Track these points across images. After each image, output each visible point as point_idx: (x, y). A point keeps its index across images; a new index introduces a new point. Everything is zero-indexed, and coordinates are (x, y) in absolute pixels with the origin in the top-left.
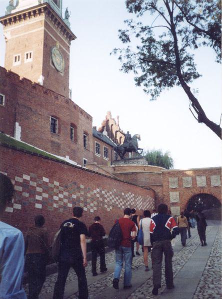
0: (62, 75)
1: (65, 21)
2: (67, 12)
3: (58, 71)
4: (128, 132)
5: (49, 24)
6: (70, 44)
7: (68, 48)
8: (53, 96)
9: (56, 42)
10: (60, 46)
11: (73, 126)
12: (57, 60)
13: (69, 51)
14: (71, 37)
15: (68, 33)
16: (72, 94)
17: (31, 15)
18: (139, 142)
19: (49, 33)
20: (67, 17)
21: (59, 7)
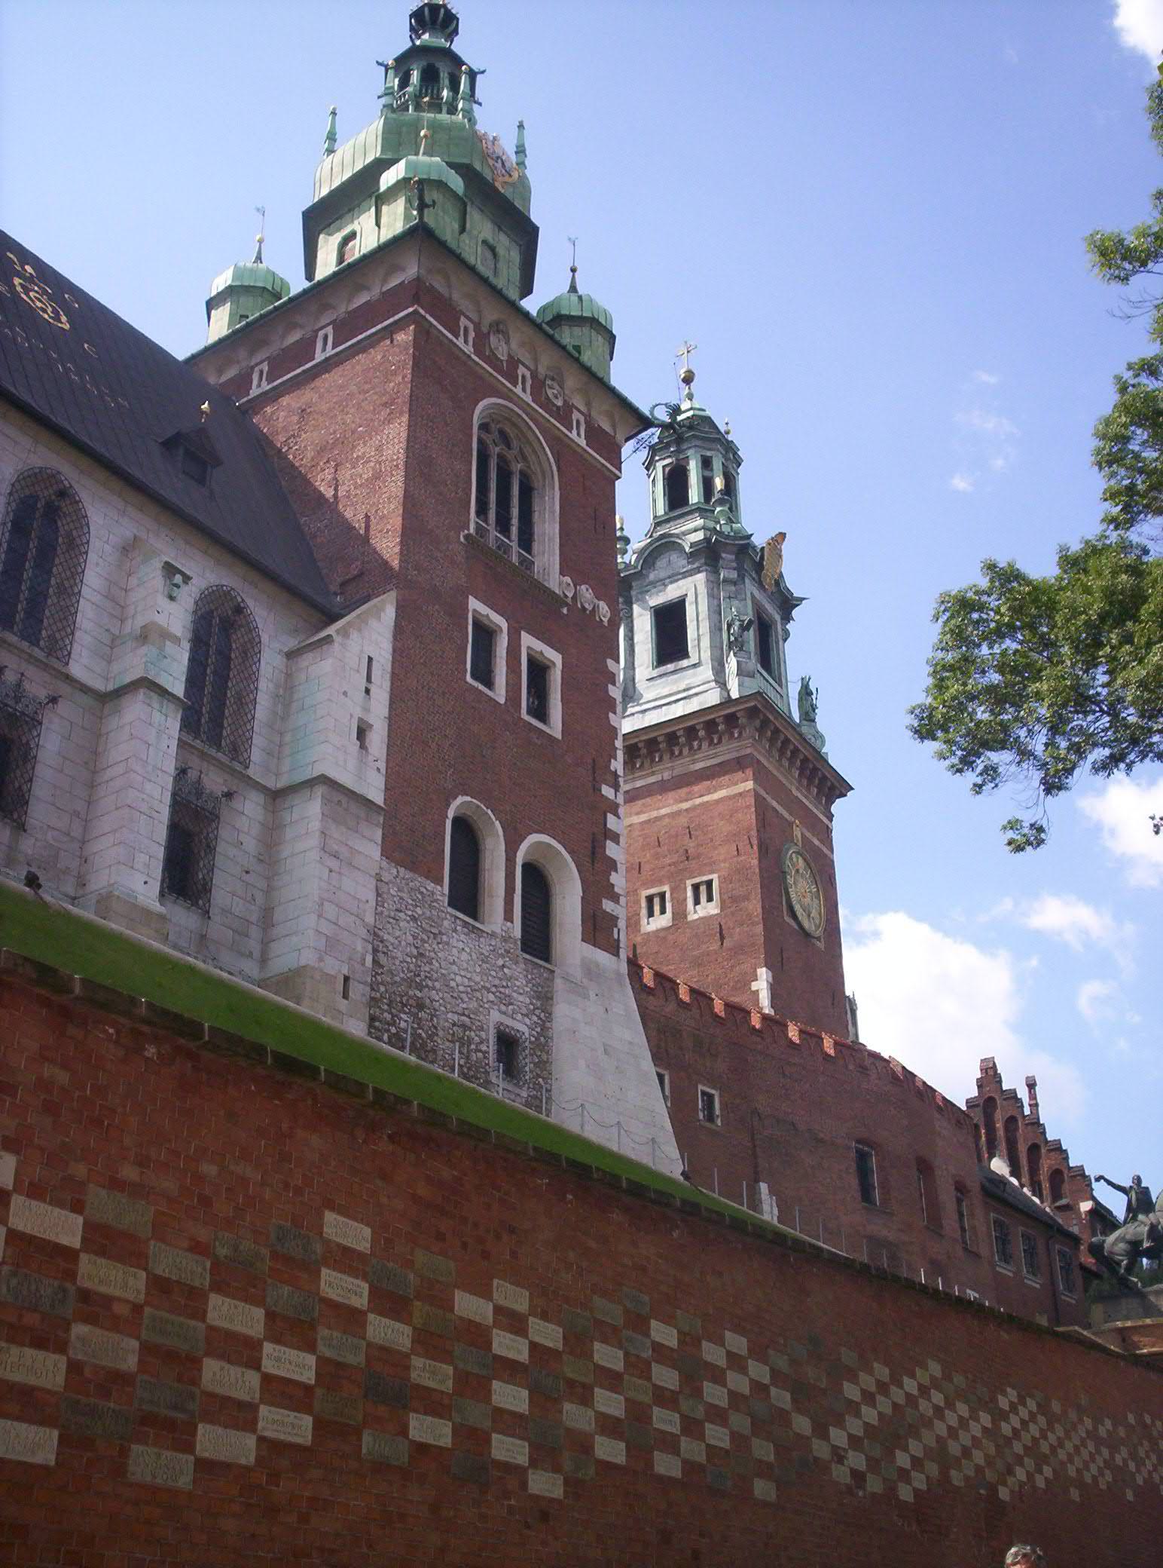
0: (821, 945)
1: (804, 730)
2: (806, 692)
3: (807, 935)
5: (766, 763)
6: (830, 817)
7: (826, 834)
8: (851, 1067)
9: (791, 824)
10: (802, 834)
11: (925, 1167)
12: (801, 890)
13: (832, 851)
14: (834, 787)
15: (824, 778)
16: (859, 1013)
17: (696, 738)
19: (769, 799)
20: (809, 713)
21: (781, 685)
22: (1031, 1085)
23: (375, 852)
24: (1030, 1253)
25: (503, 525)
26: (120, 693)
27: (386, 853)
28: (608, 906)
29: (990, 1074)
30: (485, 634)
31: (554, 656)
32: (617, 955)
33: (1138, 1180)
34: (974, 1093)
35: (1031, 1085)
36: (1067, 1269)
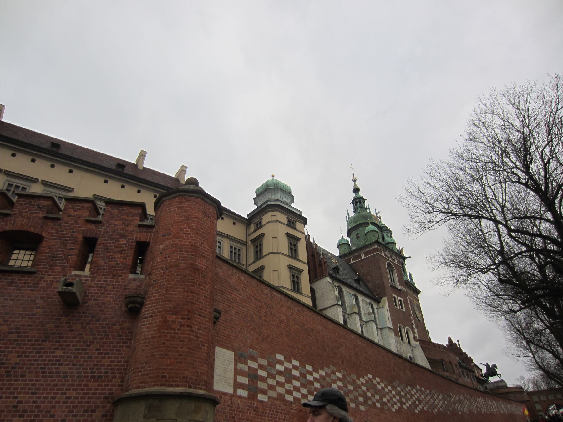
1: (411, 282)
2: (410, 275)
3: (419, 320)
4: (487, 363)
6: (418, 297)
9: (414, 301)
11: (451, 363)
14: (417, 292)
18: (497, 370)
22: (458, 341)
23: (393, 335)
24: (468, 375)
25: (392, 281)
26: (368, 322)
27: (395, 335)
28: (415, 335)
29: (450, 340)
30: (395, 298)
31: (402, 299)
32: (417, 342)
33: (487, 363)
34: (448, 343)
35: (458, 341)
36: (473, 378)
